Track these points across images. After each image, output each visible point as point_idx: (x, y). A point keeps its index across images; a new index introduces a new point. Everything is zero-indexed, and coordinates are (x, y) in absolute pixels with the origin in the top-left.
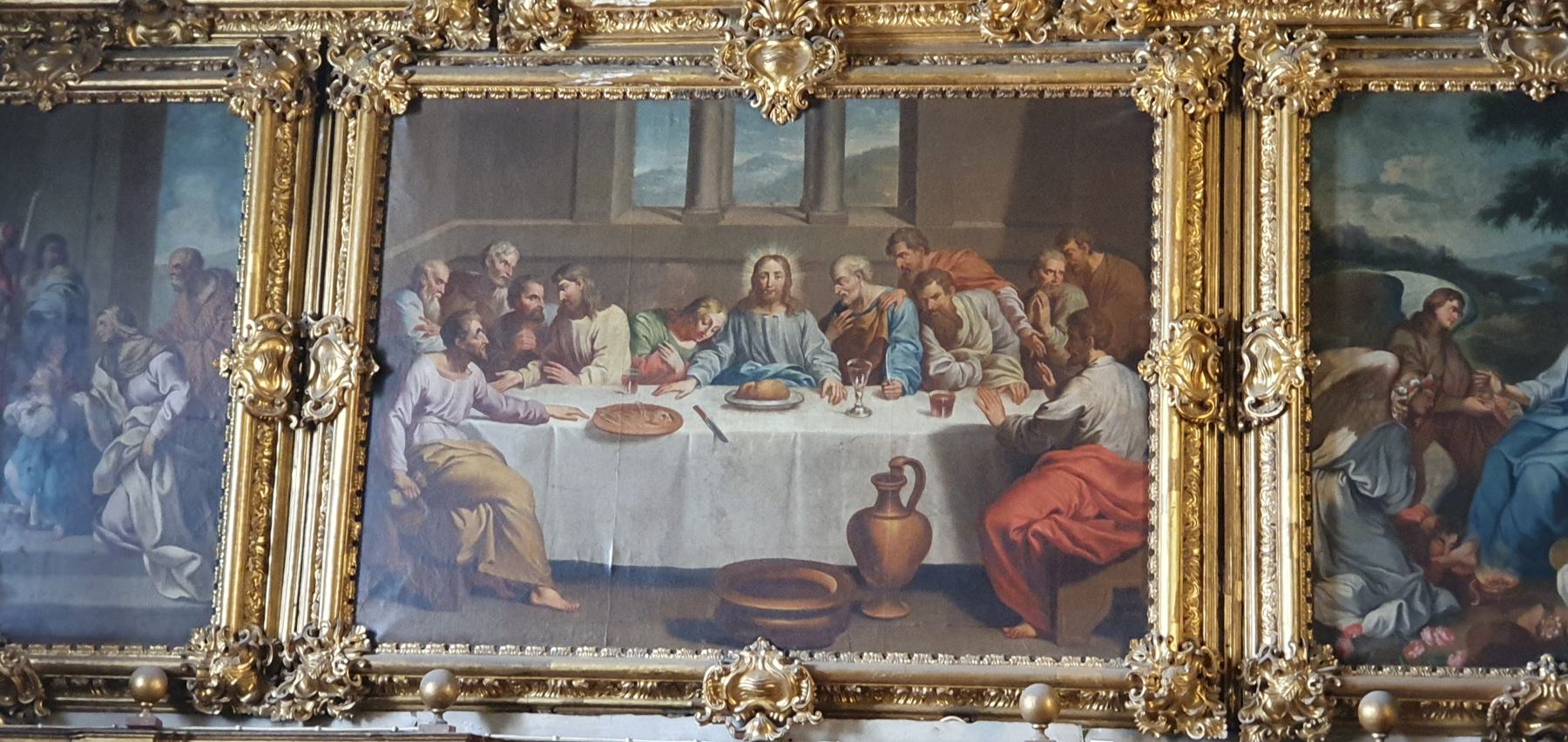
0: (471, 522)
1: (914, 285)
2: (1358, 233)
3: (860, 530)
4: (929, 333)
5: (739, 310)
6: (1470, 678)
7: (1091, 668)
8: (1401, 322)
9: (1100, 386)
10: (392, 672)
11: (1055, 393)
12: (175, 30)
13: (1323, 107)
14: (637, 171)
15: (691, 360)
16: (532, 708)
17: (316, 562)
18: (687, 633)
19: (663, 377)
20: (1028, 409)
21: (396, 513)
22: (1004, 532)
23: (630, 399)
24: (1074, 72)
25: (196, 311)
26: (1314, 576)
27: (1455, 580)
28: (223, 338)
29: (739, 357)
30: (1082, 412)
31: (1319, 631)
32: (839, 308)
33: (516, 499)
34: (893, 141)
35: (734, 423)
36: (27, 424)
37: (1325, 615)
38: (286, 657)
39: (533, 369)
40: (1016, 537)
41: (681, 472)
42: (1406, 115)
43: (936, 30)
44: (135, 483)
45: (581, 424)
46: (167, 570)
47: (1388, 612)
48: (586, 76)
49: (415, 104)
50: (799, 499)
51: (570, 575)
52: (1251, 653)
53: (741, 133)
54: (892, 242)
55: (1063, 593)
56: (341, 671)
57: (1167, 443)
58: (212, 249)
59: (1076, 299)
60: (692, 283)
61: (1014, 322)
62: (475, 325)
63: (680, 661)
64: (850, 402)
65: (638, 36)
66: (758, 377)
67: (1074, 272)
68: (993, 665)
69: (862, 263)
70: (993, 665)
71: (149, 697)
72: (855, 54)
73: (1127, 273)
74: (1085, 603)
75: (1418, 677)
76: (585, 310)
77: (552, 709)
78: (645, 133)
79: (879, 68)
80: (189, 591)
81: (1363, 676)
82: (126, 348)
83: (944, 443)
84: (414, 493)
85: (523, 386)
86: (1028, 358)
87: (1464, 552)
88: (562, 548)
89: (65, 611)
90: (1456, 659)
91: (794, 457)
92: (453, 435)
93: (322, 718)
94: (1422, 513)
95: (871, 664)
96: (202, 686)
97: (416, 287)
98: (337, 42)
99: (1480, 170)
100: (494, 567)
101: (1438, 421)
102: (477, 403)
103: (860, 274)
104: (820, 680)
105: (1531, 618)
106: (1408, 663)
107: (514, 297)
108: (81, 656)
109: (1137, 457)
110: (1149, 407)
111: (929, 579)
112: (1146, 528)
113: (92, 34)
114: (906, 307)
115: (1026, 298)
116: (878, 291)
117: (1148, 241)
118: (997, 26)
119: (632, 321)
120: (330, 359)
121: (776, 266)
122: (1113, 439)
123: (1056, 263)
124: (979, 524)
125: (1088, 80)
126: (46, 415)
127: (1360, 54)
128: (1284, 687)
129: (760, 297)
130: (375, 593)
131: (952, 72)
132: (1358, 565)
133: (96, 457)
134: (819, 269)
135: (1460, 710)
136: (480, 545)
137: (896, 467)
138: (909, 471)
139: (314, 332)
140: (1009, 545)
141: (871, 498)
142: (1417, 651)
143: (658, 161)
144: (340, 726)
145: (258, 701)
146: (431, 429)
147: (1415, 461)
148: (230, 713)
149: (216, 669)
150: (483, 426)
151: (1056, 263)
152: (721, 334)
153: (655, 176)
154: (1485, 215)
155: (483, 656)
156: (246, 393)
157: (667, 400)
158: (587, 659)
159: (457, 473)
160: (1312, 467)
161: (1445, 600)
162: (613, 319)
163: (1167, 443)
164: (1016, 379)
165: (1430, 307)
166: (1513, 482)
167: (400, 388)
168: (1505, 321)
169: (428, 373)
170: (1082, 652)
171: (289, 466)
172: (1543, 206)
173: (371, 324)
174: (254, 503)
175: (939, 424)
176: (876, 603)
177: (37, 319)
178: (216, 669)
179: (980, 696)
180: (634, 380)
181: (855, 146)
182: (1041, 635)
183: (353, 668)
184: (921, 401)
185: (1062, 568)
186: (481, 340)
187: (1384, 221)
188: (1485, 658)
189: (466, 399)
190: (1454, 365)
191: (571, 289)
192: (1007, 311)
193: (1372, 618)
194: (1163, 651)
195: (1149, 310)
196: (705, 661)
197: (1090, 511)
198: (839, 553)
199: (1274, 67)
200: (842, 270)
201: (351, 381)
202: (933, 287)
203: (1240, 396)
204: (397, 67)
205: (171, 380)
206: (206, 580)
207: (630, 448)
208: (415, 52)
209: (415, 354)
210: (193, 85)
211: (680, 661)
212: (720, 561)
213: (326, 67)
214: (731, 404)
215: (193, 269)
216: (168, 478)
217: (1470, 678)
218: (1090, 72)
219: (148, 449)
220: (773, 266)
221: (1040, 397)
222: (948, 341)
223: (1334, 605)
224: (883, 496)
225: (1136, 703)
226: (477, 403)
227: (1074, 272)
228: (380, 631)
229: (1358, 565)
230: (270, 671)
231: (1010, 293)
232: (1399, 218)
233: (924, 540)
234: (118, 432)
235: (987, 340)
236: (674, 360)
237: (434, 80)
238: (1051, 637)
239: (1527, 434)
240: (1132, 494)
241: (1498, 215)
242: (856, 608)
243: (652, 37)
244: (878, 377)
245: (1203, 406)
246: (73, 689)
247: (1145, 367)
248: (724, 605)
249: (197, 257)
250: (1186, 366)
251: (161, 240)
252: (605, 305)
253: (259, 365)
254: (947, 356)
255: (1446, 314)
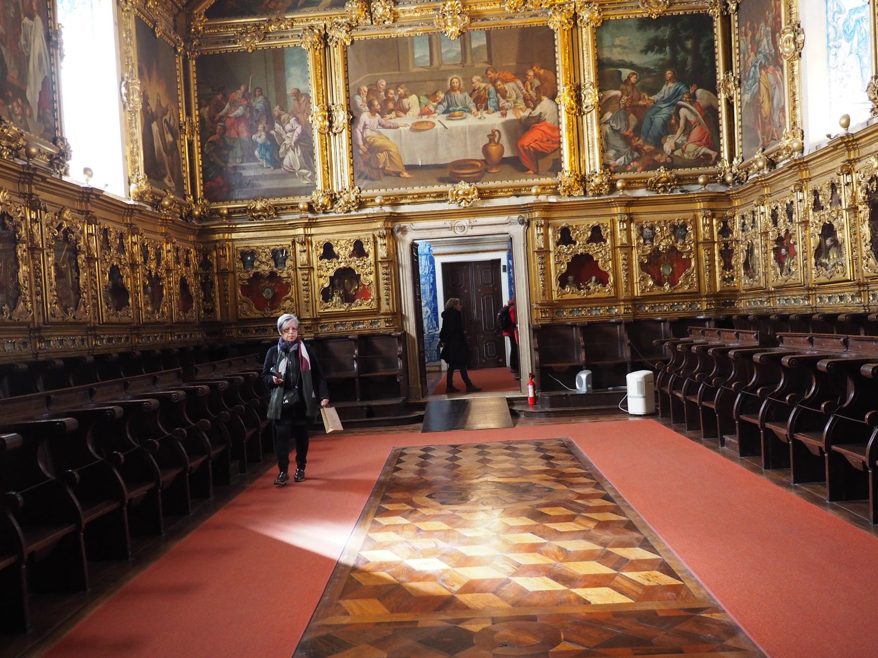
0: (382, 157)
1: (493, 82)
2: (609, 59)
3: (485, 149)
4: (499, 95)
5: (447, 93)
6: (643, 174)
7: (548, 180)
8: (621, 82)
9: (545, 106)
10: (366, 198)
11: (534, 109)
12: (283, 26)
13: (599, 25)
14: (416, 56)
15: (436, 108)
16: (403, 204)
17: (342, 171)
18: (443, 180)
19: (429, 113)
20: (526, 114)
21: (361, 155)
22: (523, 147)
23: (421, 120)
24: (532, 19)
25: (300, 105)
26: (603, 151)
27: (638, 149)
28: (308, 111)
29: (449, 106)
30: (541, 113)
31: (605, 166)
32: (474, 90)
33: (393, 150)
34: (484, 42)
35: (449, 124)
36: (260, 141)
37: (606, 161)
38: (338, 196)
39: (394, 113)
40: (526, 148)
41: (437, 138)
42: (620, 25)
43: (493, 10)
44: (291, 154)
45: (408, 128)
46: (303, 176)
47: (622, 159)
48: (399, 30)
49: (352, 42)
50: (469, 143)
51: (410, 168)
52: (588, 172)
53: (443, 44)
54: (487, 71)
55: (540, 162)
56: (353, 198)
57: (564, 120)
58: (302, 88)
59: (537, 83)
60: (434, 87)
61: (521, 90)
62: (376, 103)
63: (442, 188)
64: (480, 116)
65: (411, 17)
66: (454, 111)
67: (535, 75)
68: (523, 182)
69: (479, 78)
70: (523, 182)
71: (305, 210)
72: (473, 19)
73: (550, 75)
74: (545, 164)
75: (631, 175)
76: (406, 96)
77: (409, 204)
78: (417, 46)
79: (479, 22)
80: (309, 181)
81: (617, 176)
82: (283, 117)
83: (505, 124)
84: (366, 150)
85: (391, 119)
86: (525, 100)
87: (640, 142)
88: (407, 162)
89: (277, 189)
90: (640, 169)
91: (466, 132)
92: (374, 134)
93: (349, 211)
94: (629, 133)
95: (491, 184)
96: (317, 206)
97: (359, 94)
98: (328, 26)
99: (640, 39)
100: (389, 168)
101: (633, 108)
102: (380, 124)
103: (479, 80)
104: (479, 189)
105: (657, 157)
106: (628, 172)
107: (386, 94)
108: (283, 200)
109: (556, 124)
110: (558, 111)
111: (504, 161)
112: (560, 143)
113: (259, 29)
114: (492, 89)
115: (524, 83)
116: (484, 85)
117: (555, 65)
118: (511, 8)
119: (419, 98)
120: (339, 115)
121: (456, 80)
122: (550, 120)
123: (531, 73)
124: (516, 145)
125: (537, 21)
126: (263, 137)
127: (607, 9)
128: (597, 181)
129: (453, 89)
130: (359, 177)
131: (499, 21)
132: (614, 147)
133: (279, 148)
134: (468, 80)
135: (641, 182)
136: (385, 163)
137: (493, 132)
138: (497, 133)
139: (333, 108)
140: (525, 150)
141: (487, 141)
142: (630, 168)
143: (421, 53)
144: (352, 213)
145: (332, 208)
146: (368, 133)
147: (627, 119)
148: (324, 212)
149: (320, 201)
150: (382, 130)
151: (531, 73)
152: (443, 100)
153: (421, 58)
154: (642, 52)
155: (390, 191)
156: (318, 126)
157: (431, 119)
158: (417, 190)
159: (376, 144)
160: (600, 124)
161: (636, 154)
162: (413, 99)
163: (564, 120)
164: (523, 106)
165: (629, 77)
166: (652, 122)
167: (358, 122)
168: (648, 80)
169: (365, 117)
170: (546, 176)
171: (330, 146)
172: (657, 48)
173: (348, 105)
174: (323, 157)
175: (504, 119)
176: (491, 169)
177: (257, 111)
178: (320, 201)
179: (520, 190)
180: (422, 114)
181: (474, 45)
182: (535, 173)
183: (356, 198)
184: (498, 114)
185: (539, 155)
186: (379, 107)
187: (615, 55)
188: (646, 169)
189: (377, 123)
190: (636, 93)
191: (401, 91)
192: (519, 88)
193: (618, 161)
194: (567, 174)
195: (557, 84)
196: (449, 187)
197: (545, 140)
198: (480, 156)
199: (585, 15)
200: (474, 80)
201: (346, 121)
202: (499, 83)
203: (581, 106)
204: (347, 32)
205: (296, 125)
206: (313, 178)
207: (422, 133)
208: (351, 27)
209: (360, 112)
210: (290, 42)
211: (442, 188)
212: (450, 161)
213: (326, 34)
214: (448, 119)
215: (298, 94)
216: (299, 151)
217: (643, 174)
218: (537, 19)
219: (293, 144)
220: (455, 80)
221: (530, 110)
222: (504, 97)
223: (608, 158)
224: (490, 140)
225: (560, 189)
226: (380, 124)
227: (536, 75)
228: (361, 187)
229: (614, 147)
230: (334, 200)
231: (519, 82)
232: (620, 54)
233: (503, 152)
234: (284, 140)
235: (514, 96)
236: (431, 108)
237: (358, 35)
238: (537, 173)
239: (654, 110)
240: (556, 134)
241: (645, 51)
242: (486, 170)
243: (415, 17)
244: (486, 108)
245: (572, 109)
246: (282, 209)
247: (557, 100)
248: (452, 172)
249: (298, 90)
250: (568, 99)
251: (287, 87)
252: (411, 94)
253: (320, 119)
254: (504, 101)
255: (633, 79)
